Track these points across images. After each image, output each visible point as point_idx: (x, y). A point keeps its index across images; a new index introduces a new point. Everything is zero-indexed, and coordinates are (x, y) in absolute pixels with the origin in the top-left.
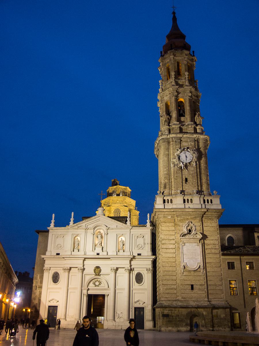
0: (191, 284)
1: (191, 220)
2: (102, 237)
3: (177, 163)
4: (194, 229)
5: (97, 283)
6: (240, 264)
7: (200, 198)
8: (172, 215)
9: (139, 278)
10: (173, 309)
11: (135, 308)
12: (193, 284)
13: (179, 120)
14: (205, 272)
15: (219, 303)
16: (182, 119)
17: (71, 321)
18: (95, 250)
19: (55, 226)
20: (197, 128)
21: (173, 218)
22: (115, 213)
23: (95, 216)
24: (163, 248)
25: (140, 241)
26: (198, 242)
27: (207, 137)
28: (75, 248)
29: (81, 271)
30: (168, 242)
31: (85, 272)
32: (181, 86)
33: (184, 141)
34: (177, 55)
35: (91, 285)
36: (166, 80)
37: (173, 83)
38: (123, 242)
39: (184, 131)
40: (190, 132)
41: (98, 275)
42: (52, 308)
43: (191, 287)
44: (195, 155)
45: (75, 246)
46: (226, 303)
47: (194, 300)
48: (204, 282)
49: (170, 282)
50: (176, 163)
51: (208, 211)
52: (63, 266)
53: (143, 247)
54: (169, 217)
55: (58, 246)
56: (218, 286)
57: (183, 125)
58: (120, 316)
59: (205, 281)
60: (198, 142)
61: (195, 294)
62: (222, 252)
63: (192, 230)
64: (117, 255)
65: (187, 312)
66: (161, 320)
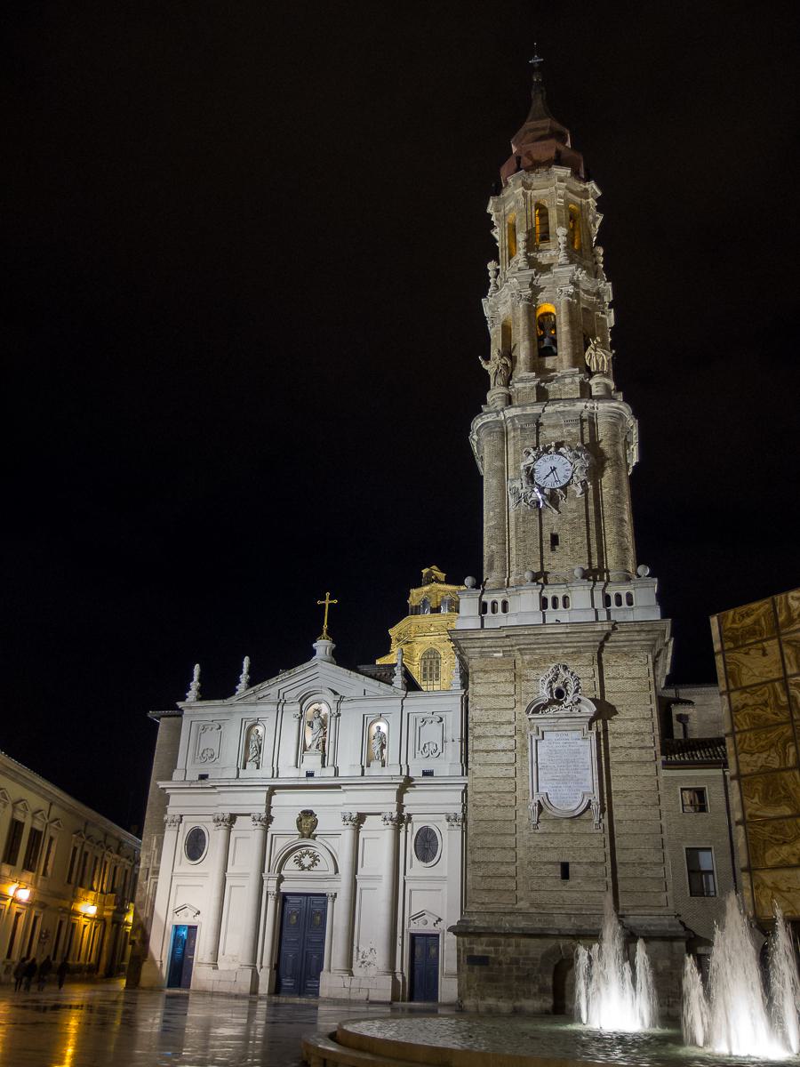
0: (563, 861)
1: (563, 661)
3: (524, 490)
4: (571, 687)
5: (307, 861)
6: (723, 795)
7: (592, 591)
8: (508, 649)
9: (427, 846)
10: (502, 940)
12: (570, 860)
13: (537, 368)
14: (606, 821)
15: (651, 922)
16: (549, 362)
19: (200, 699)
20: (592, 382)
21: (510, 656)
22: (425, 662)
23: (304, 665)
24: (476, 751)
26: (586, 727)
27: (621, 407)
28: (250, 758)
30: (494, 732)
31: (273, 827)
32: (546, 269)
33: (549, 426)
36: (507, 259)
37: (521, 265)
43: (559, 871)
44: (583, 462)
45: (251, 749)
46: (677, 922)
47: (569, 912)
48: (602, 853)
49: (497, 856)
50: (522, 491)
51: (614, 628)
53: (440, 749)
54: (495, 655)
56: (648, 866)
57: (551, 380)
58: (367, 960)
59: (608, 849)
60: (593, 425)
61: (575, 895)
62: (664, 757)
63: (567, 691)
64: (363, 775)
65: (544, 950)
66: (465, 975)
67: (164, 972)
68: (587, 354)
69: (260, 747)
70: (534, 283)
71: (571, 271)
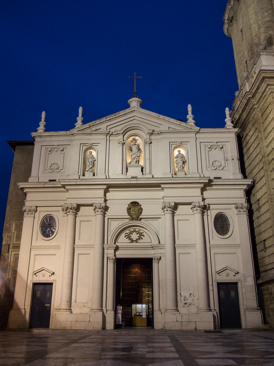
2: (139, 149)
5: (135, 236)
11: (219, 284)
17: (82, 314)
18: (127, 171)
23: (126, 110)
25: (217, 155)
28: (86, 170)
29: (100, 211)
31: (109, 214)
35: (123, 240)
38: (182, 157)
41: (137, 220)
42: (42, 287)
52: (62, 203)
55: (52, 168)
58: (189, 301)
67: (27, 317)
69: (94, 163)
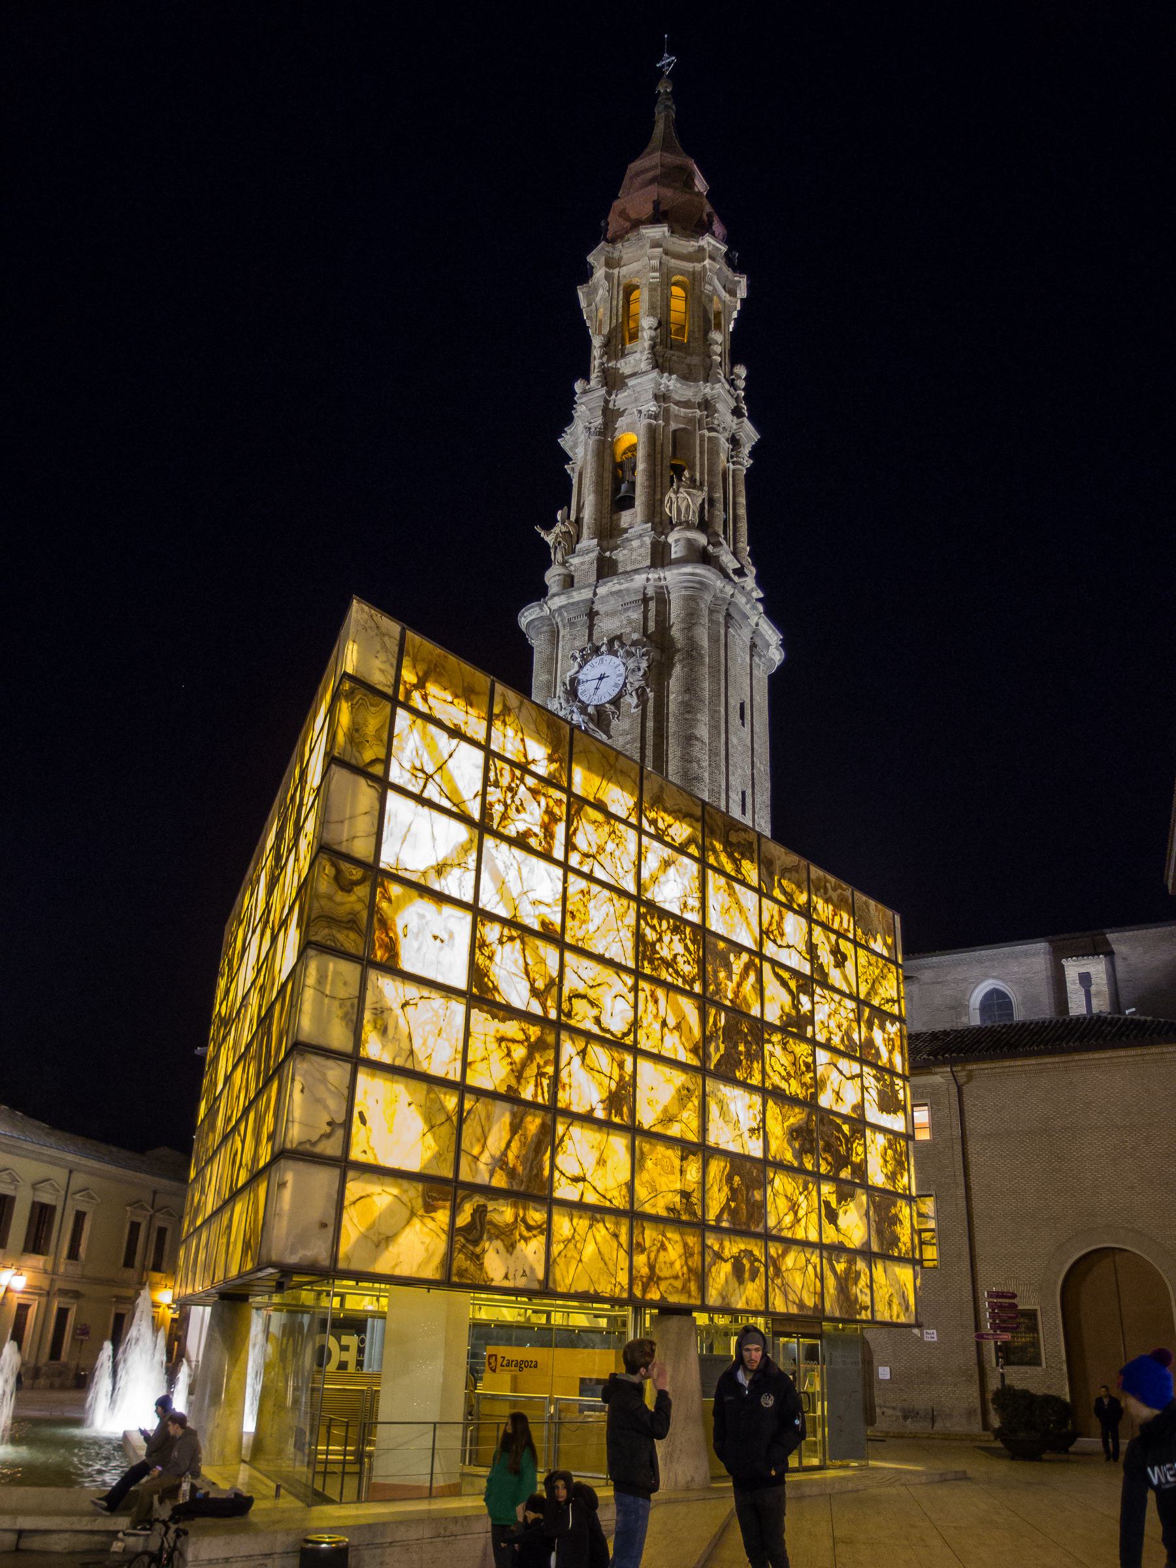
16: (626, 518)
20: (671, 540)
27: (698, 571)
34: (625, 257)
39: (620, 571)
40: (638, 566)
68: (667, 498)
70: (611, 406)
71: (652, 379)
